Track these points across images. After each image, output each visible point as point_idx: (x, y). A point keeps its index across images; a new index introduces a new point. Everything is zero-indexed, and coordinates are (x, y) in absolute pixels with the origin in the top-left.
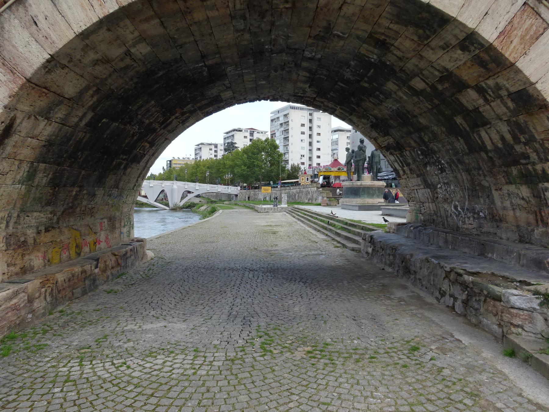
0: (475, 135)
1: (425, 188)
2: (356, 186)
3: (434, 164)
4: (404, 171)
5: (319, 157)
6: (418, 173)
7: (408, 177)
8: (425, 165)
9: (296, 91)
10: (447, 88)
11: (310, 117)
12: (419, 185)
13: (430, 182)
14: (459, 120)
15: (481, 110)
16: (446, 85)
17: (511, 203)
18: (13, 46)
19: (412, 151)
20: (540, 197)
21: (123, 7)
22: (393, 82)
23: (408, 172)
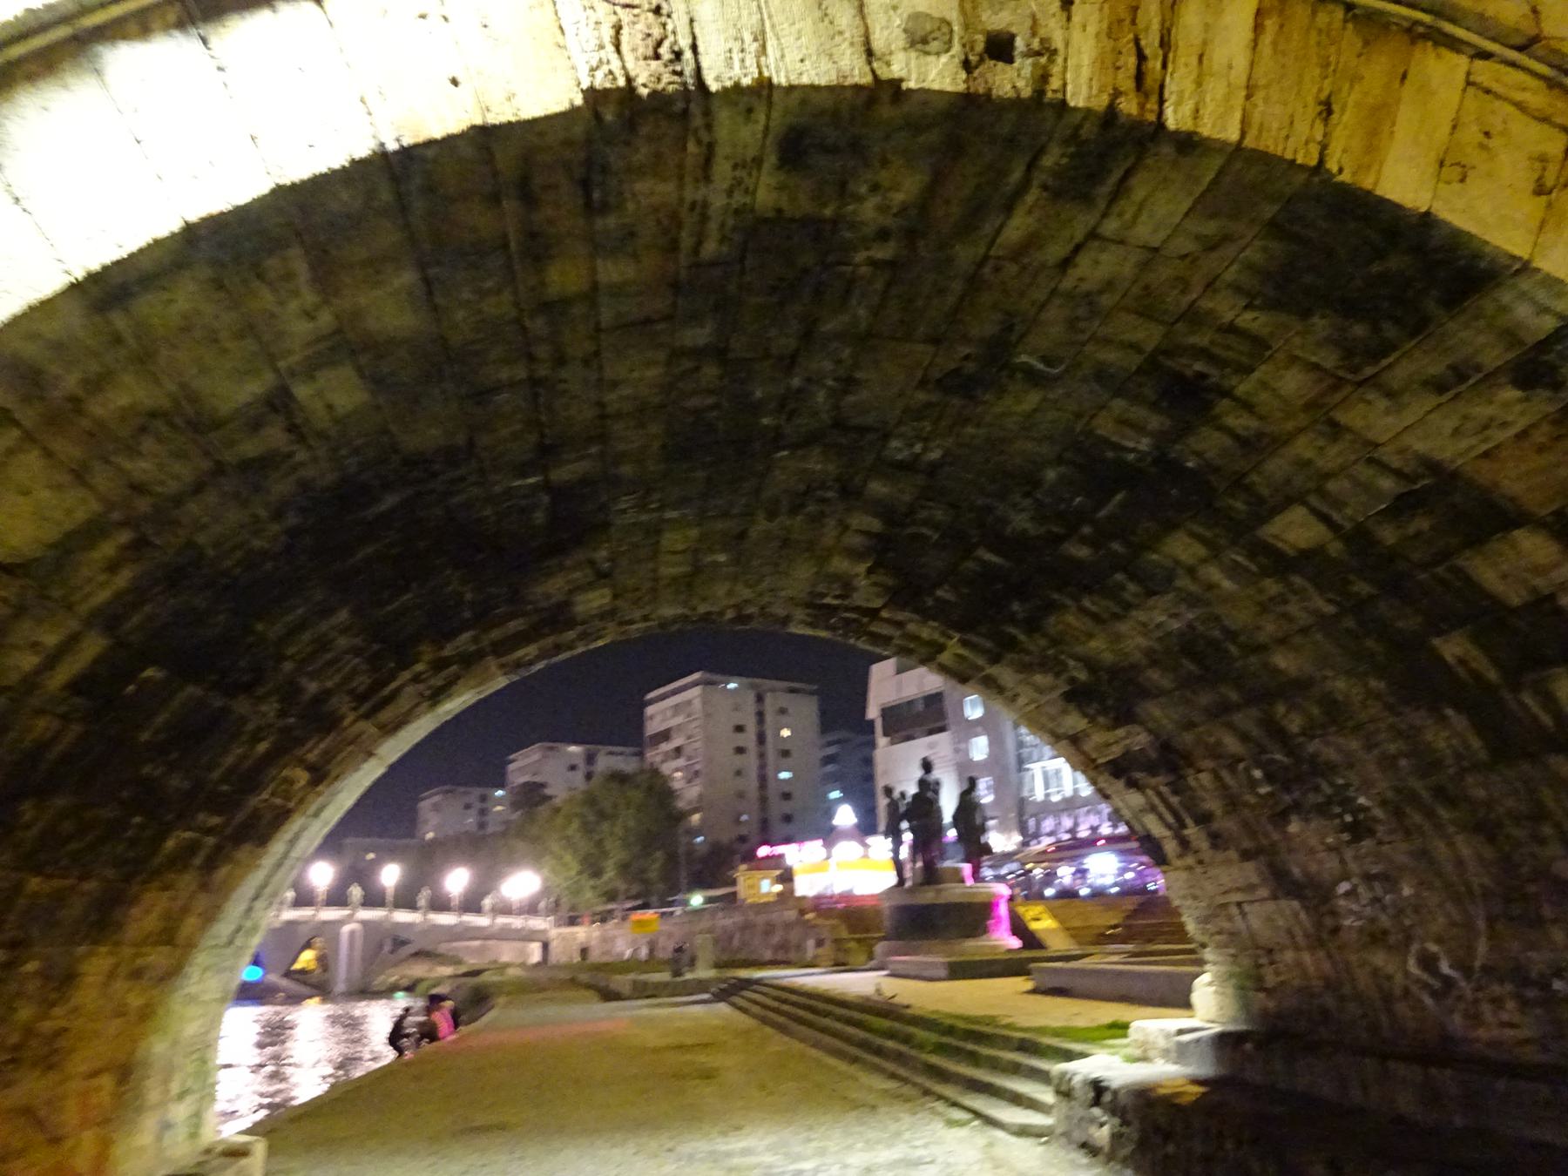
0: (1528, 699)
1: (1275, 897)
3: (1322, 810)
4: (1184, 844)
6: (1247, 844)
7: (1201, 862)
8: (1281, 817)
9: (821, 588)
10: (1418, 534)
12: (1251, 888)
14: (1452, 648)
16: (1422, 523)
19: (1225, 774)
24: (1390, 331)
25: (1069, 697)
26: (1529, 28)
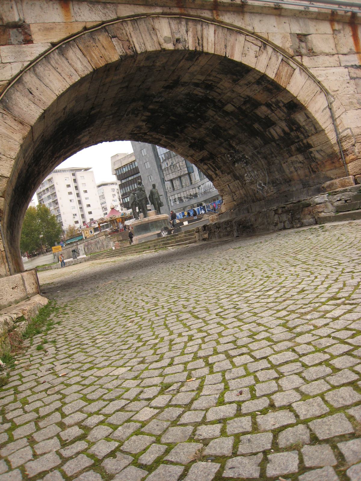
2: (144, 223)
4: (216, 174)
5: (90, 213)
6: (228, 171)
11: (73, 177)
14: (256, 126)
15: (269, 116)
17: (294, 167)
18: (20, 108)
19: (223, 157)
20: (309, 158)
21: (84, 77)
23: (220, 174)
24: (239, 77)
25: (190, 146)
26: (252, 31)
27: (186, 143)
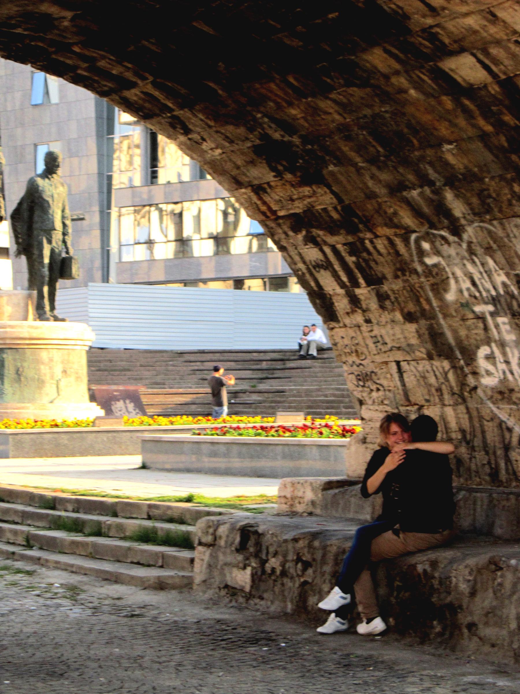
1: (430, 357)
4: (355, 301)
6: (411, 307)
7: (368, 321)
12: (410, 349)
13: (452, 341)
19: (398, 241)
22: (386, 51)
23: (373, 305)
25: (257, 150)
27: (241, 131)
